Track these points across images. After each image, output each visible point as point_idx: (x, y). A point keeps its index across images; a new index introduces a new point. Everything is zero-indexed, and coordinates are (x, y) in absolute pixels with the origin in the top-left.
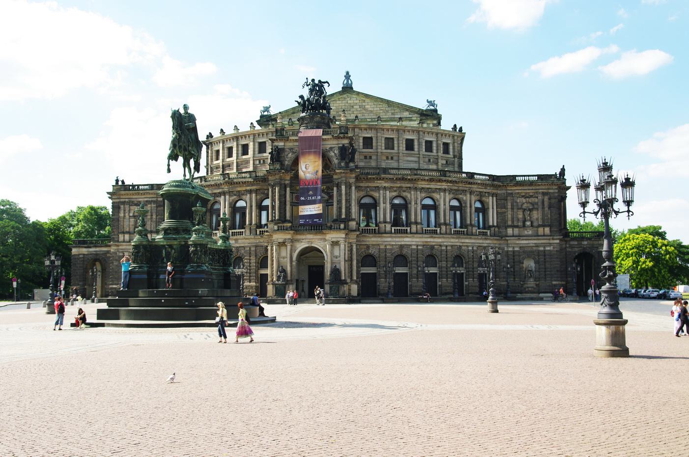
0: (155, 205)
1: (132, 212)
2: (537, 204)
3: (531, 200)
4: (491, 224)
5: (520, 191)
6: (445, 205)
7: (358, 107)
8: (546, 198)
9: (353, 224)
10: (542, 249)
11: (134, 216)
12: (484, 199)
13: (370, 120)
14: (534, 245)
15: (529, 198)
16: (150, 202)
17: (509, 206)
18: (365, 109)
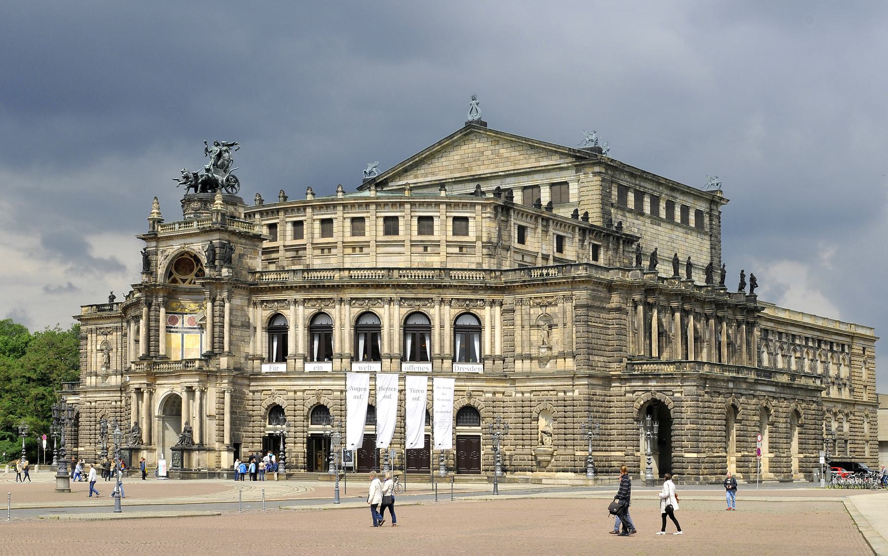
0: (120, 333)
1: (99, 343)
2: (556, 315)
3: (549, 310)
4: (487, 352)
5: (533, 295)
6: (391, 326)
7: (489, 153)
8: (569, 306)
9: (224, 362)
10: (561, 394)
11: (102, 350)
12: (473, 311)
13: (503, 173)
14: (551, 388)
15: (546, 306)
16: (117, 329)
17: (518, 322)
18: (498, 155)
